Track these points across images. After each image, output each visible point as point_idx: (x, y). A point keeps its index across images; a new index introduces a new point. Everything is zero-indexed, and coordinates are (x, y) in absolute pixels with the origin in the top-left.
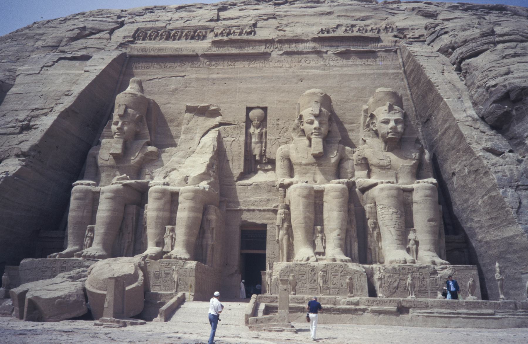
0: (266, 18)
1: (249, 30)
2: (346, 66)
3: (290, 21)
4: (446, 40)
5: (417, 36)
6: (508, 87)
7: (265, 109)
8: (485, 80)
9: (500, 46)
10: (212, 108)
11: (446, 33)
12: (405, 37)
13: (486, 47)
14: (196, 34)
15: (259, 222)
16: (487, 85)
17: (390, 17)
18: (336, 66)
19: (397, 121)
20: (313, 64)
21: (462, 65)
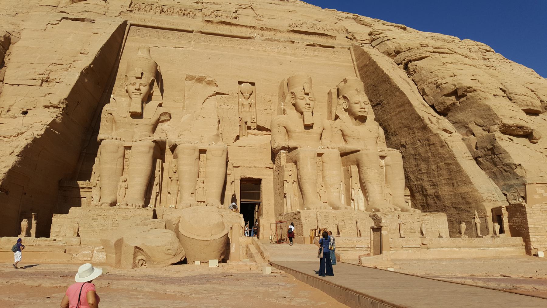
1: (234, 15)
4: (391, 46)
6: (458, 86)
7: (253, 84)
8: (436, 79)
11: (388, 40)
12: (355, 38)
13: (428, 54)
15: (256, 177)
17: (339, 22)
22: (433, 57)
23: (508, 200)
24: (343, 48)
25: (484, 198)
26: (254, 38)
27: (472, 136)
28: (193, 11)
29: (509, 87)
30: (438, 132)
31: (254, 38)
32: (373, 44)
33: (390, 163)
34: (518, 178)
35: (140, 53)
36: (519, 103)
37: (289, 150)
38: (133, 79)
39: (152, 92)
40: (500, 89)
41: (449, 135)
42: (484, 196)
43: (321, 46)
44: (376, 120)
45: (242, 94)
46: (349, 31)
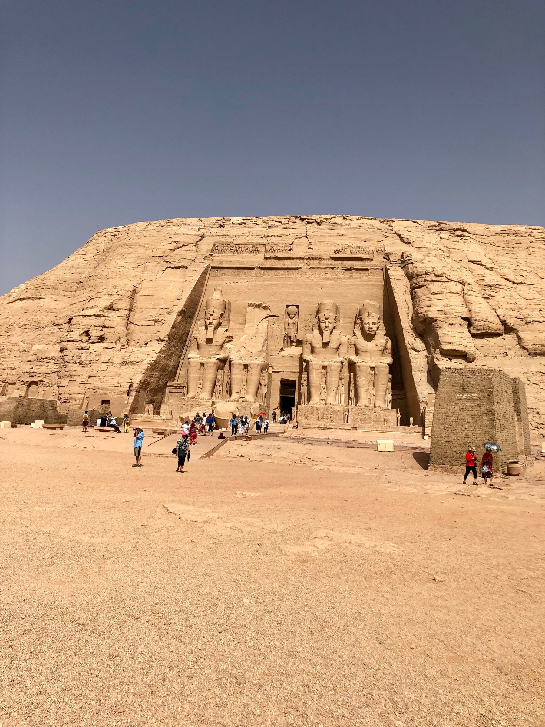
1: (289, 248)
2: (349, 278)
3: (317, 240)
5: (396, 260)
7: (297, 306)
10: (265, 305)
11: (412, 263)
12: (389, 259)
13: (426, 283)
14: (253, 249)
18: (344, 279)
19: (373, 323)
20: (329, 276)
22: (428, 286)
25: (421, 399)
26: (301, 268)
29: (473, 315)
30: (409, 351)
31: (301, 268)
33: (377, 372)
35: (214, 294)
38: (208, 316)
39: (221, 321)
45: (288, 314)
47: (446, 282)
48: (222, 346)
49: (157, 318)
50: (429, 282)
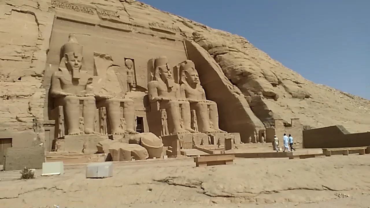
0: (121, 9)
1: (117, 15)
2: (164, 44)
5: (190, 37)
6: (243, 71)
7: (133, 60)
8: (232, 66)
9: (231, 52)
10: (107, 56)
11: (204, 39)
12: (185, 36)
13: (227, 51)
14: (87, 10)
16: (234, 68)
17: (174, 23)
20: (151, 41)
21: (217, 56)
23: (265, 127)
24: (179, 41)
26: (131, 31)
27: (249, 96)
28: (92, 9)
29: (265, 72)
30: (235, 93)
31: (131, 31)
32: (196, 40)
34: (270, 116)
36: (270, 80)
37: (161, 101)
38: (73, 58)
40: (262, 73)
41: (239, 95)
42: (256, 125)
43: (168, 39)
44: (201, 85)
45: (126, 65)
46: (182, 31)
47: (238, 52)
48: (86, 86)
49: (23, 54)
50: (229, 51)
